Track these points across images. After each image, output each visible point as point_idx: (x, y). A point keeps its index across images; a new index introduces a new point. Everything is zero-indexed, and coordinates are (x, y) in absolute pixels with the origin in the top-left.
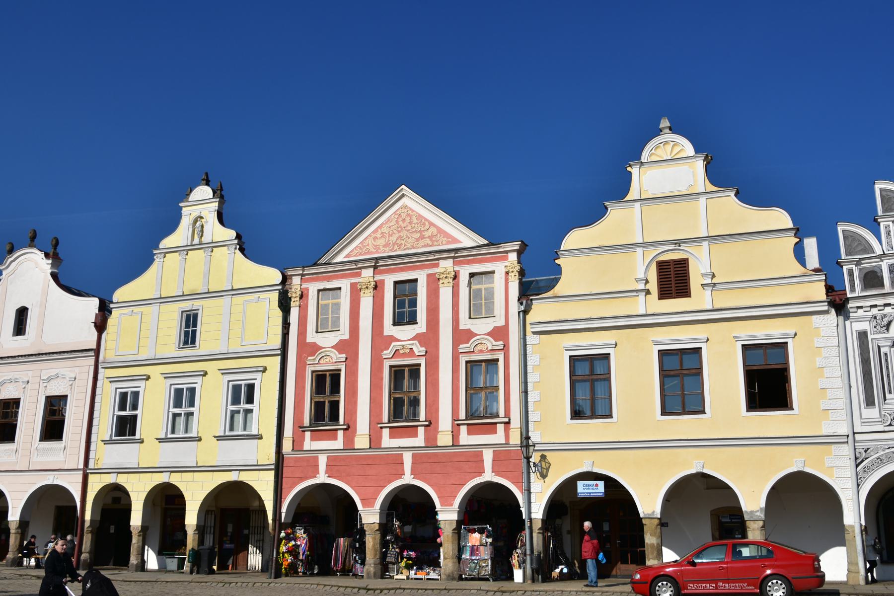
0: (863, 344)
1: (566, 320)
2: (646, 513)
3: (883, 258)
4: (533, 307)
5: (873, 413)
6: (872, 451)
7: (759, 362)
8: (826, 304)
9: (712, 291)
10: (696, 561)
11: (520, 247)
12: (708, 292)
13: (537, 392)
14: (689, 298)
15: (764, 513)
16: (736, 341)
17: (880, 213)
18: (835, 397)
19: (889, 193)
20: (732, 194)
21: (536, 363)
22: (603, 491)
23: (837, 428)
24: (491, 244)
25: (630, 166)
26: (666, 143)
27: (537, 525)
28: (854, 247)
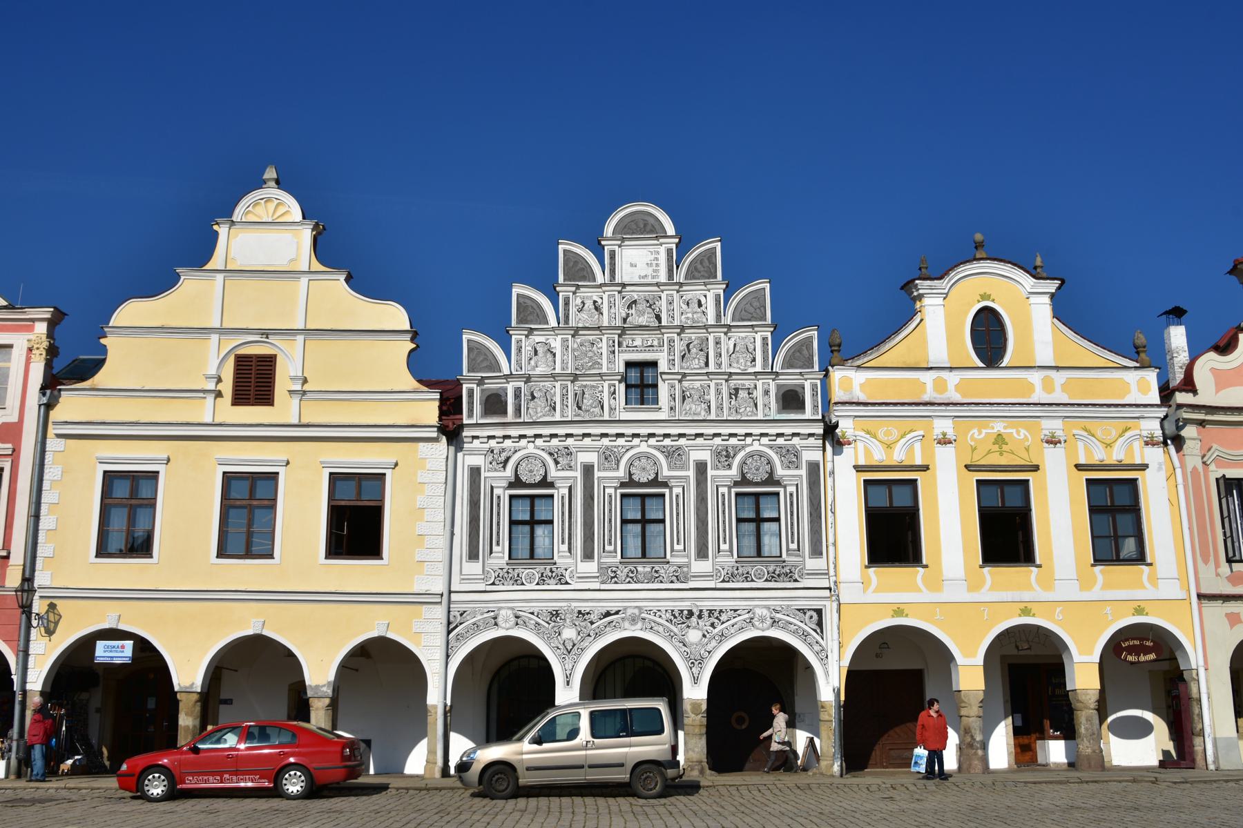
0: (474, 482)
1: (103, 421)
2: (182, 685)
3: (509, 380)
4: (61, 400)
5: (475, 568)
6: (469, 614)
7: (348, 496)
8: (436, 429)
9: (300, 400)
10: (200, 746)
11: (52, 315)
12: (295, 401)
13: (53, 518)
14: (271, 407)
15: (332, 688)
16: (323, 467)
17: (514, 323)
18: (433, 547)
19: (526, 301)
20: (342, 278)
21: (55, 478)
22: (130, 655)
23: (432, 585)
24: (10, 307)
25: (217, 224)
26: (268, 200)
27: (35, 700)
28: (478, 361)
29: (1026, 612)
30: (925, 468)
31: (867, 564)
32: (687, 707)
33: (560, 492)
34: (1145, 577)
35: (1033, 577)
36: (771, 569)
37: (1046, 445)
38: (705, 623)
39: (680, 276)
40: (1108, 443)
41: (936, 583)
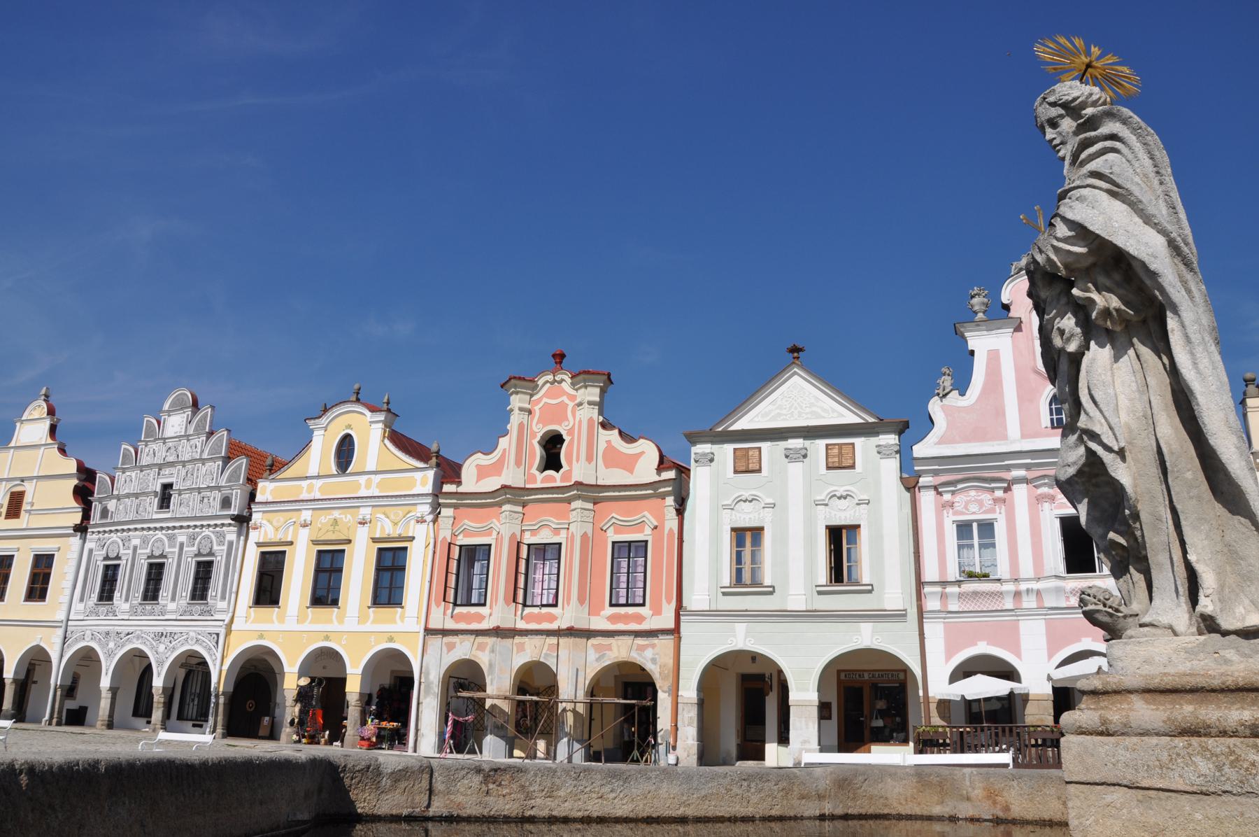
5: (78, 606)
29: (327, 638)
30: (291, 543)
31: (251, 605)
32: (154, 691)
33: (122, 563)
34: (398, 615)
35: (335, 614)
36: (202, 608)
37: (359, 525)
38: (167, 640)
39: (191, 431)
40: (396, 522)
41: (281, 619)
